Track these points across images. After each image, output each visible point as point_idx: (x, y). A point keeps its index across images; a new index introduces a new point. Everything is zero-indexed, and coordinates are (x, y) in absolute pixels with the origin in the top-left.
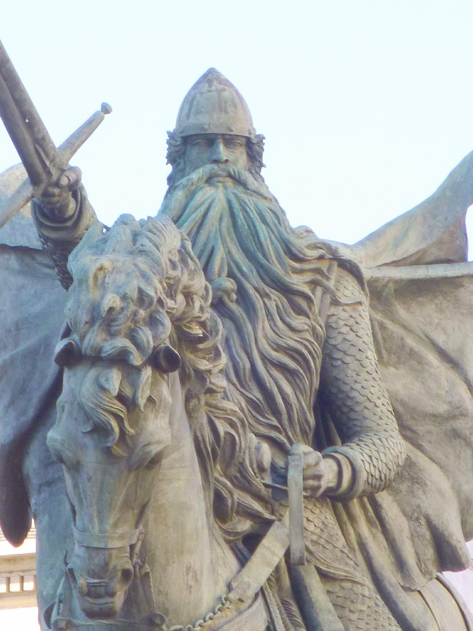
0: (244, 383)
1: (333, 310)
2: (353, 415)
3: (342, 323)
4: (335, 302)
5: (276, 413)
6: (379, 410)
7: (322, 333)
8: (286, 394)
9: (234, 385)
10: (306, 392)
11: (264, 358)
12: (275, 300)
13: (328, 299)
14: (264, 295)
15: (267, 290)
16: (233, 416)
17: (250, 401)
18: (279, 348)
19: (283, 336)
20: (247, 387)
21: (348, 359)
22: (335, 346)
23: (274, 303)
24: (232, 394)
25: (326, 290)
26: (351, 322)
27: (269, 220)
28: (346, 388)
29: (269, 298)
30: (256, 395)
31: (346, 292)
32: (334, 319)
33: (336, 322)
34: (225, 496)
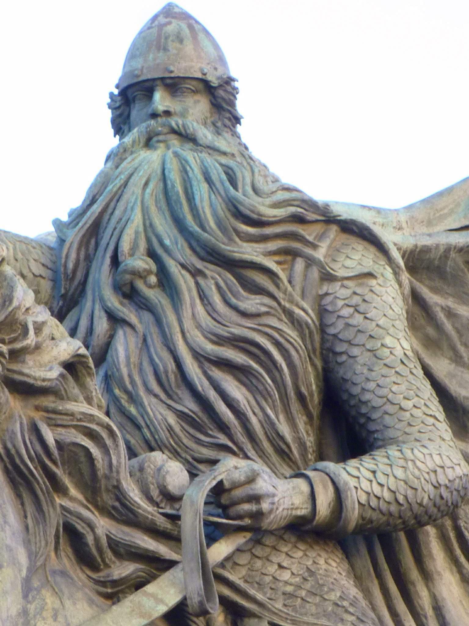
0: (170, 392)
1: (325, 288)
2: (372, 427)
3: (340, 303)
4: (328, 277)
5: (223, 428)
6: (408, 414)
7: (310, 321)
8: (233, 399)
9: (156, 396)
10: (270, 396)
12: (213, 278)
13: (315, 273)
14: (196, 273)
15: (199, 265)
16: (90, 421)
17: (182, 416)
18: (220, 340)
19: (227, 324)
20: (175, 397)
21: (355, 351)
22: (335, 336)
23: (213, 282)
24: (154, 409)
25: (310, 262)
26: (356, 300)
27: (214, 177)
28: (355, 390)
29: (204, 276)
30: (190, 405)
31: (348, 263)
32: (329, 299)
33: (332, 303)
34: (81, 530)
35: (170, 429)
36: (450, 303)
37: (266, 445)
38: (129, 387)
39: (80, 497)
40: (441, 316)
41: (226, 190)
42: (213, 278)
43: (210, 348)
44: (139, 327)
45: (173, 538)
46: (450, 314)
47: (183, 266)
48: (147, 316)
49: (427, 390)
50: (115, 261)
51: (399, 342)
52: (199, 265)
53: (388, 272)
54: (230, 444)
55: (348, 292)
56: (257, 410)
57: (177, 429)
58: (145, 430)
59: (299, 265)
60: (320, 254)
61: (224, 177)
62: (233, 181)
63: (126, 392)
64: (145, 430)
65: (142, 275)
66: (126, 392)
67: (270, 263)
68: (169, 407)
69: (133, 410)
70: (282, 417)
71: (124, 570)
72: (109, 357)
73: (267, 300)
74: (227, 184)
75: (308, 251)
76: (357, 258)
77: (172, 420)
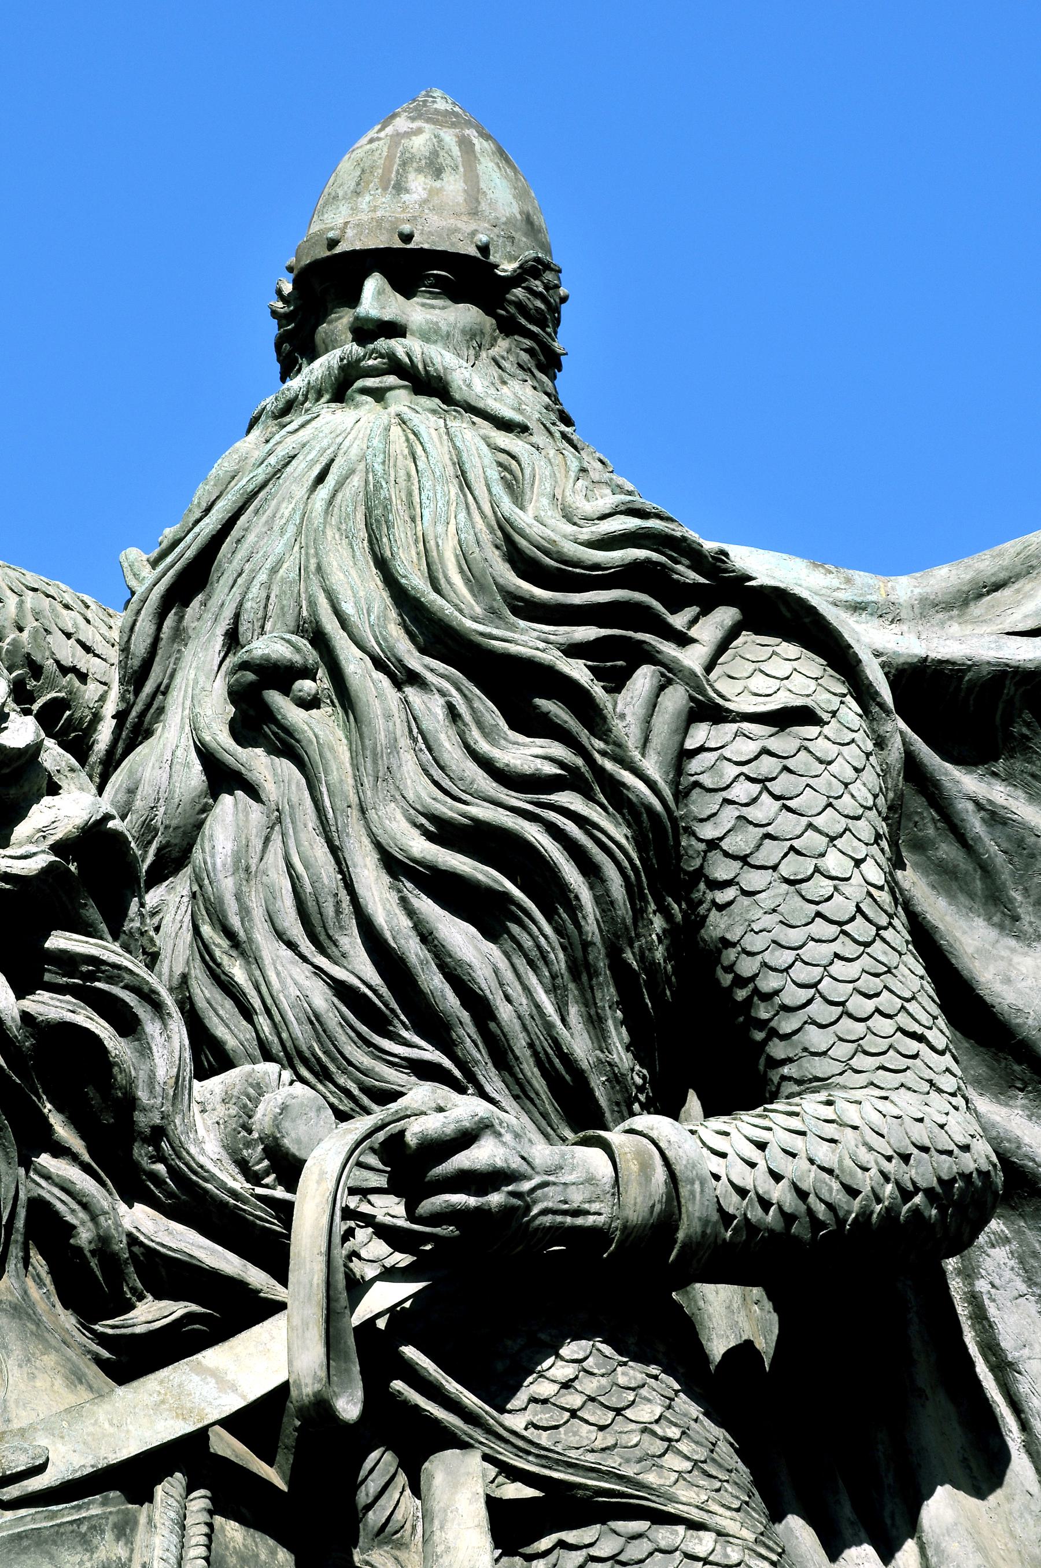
0: (323, 937)
1: (700, 734)
7: (658, 806)
8: (460, 962)
9: (291, 945)
10: (547, 963)
11: (394, 865)
12: (442, 693)
13: (675, 699)
14: (405, 678)
15: (416, 661)
16: (110, 980)
17: (342, 990)
18: (443, 832)
19: (465, 797)
20: (332, 950)
23: (441, 701)
24: (284, 974)
25: (670, 674)
26: (767, 766)
30: (361, 969)
32: (705, 759)
34: (69, 1218)
35: (315, 1020)
36: (999, 793)
37: (530, 1070)
38: (235, 922)
39: (78, 1145)
40: (976, 825)
41: (494, 505)
42: (442, 693)
43: (421, 848)
44: (270, 789)
45: (273, 1253)
46: (995, 817)
47: (379, 664)
48: (286, 766)
49: (912, 975)
50: (233, 639)
51: (854, 867)
52: (416, 661)
53: (851, 711)
54: (447, 1063)
55: (750, 748)
56: (515, 990)
57: (332, 1021)
58: (262, 1020)
59: (644, 678)
60: (693, 658)
61: (494, 473)
62: (514, 488)
63: (229, 934)
64: (262, 1020)
65: (281, 675)
66: (229, 934)
67: (578, 670)
68: (319, 971)
69: (238, 972)
70: (574, 1012)
71: (150, 1314)
72: (197, 855)
73: (558, 750)
74: (498, 489)
75: (669, 649)
76: (773, 672)
77: (321, 998)
